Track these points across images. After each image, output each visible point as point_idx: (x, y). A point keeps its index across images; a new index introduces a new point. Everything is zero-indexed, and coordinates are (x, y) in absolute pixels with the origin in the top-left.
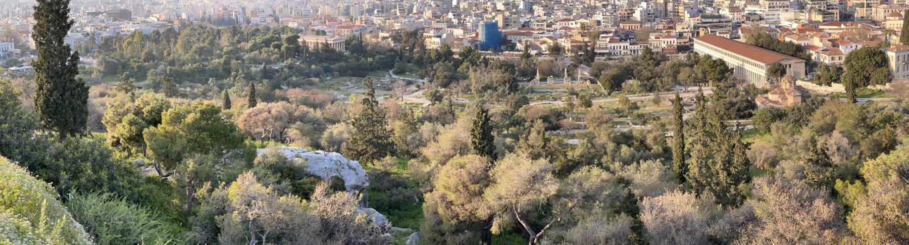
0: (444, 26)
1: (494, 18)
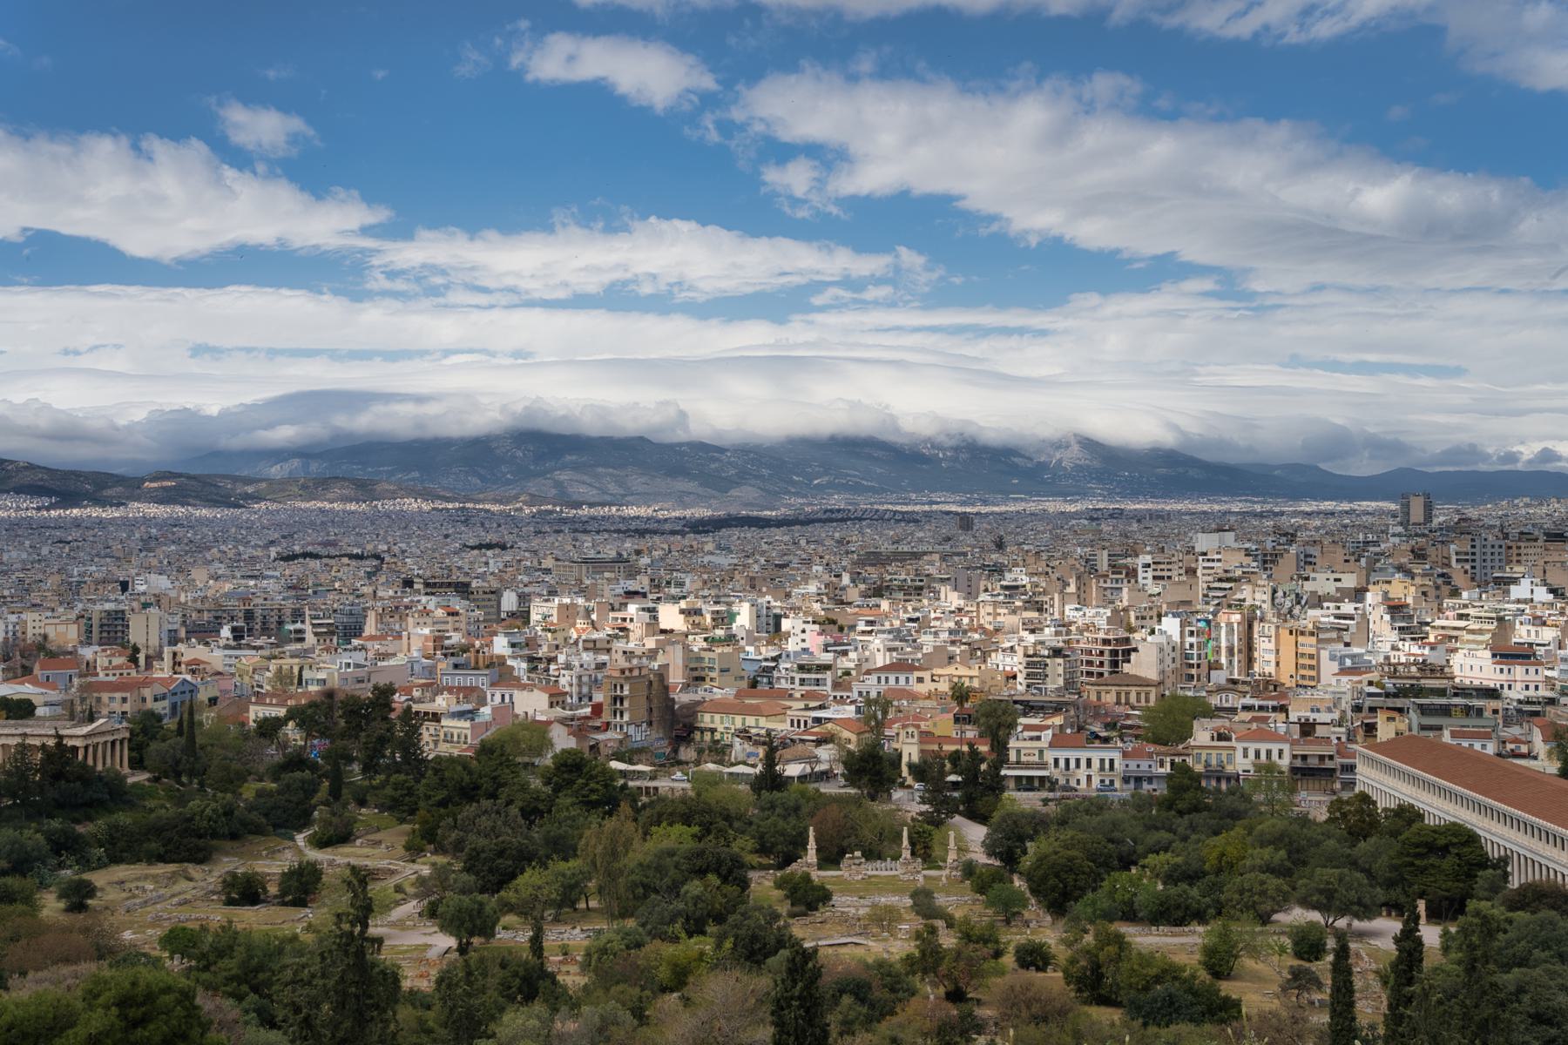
0: (481, 680)
1: (652, 655)
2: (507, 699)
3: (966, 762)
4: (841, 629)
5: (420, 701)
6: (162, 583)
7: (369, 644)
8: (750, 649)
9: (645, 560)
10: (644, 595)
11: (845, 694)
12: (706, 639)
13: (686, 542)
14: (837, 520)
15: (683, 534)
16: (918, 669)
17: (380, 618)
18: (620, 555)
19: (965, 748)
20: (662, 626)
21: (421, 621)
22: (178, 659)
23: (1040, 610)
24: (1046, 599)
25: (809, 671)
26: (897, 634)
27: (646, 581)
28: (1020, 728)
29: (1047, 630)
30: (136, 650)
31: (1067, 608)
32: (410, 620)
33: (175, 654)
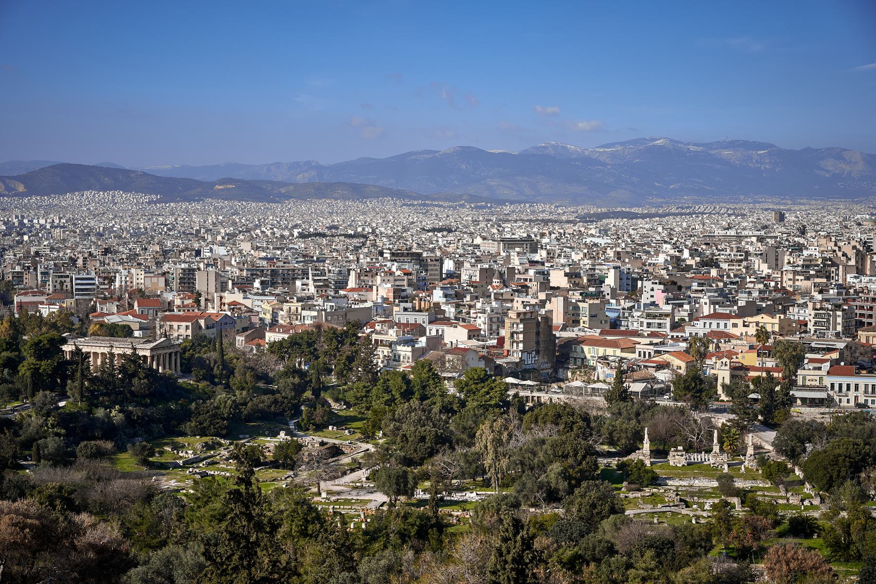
0: (422, 318)
1: (543, 303)
2: (440, 333)
3: (765, 384)
4: (680, 288)
5: (379, 333)
6: (221, 251)
7: (350, 294)
8: (613, 301)
9: (545, 240)
10: (543, 264)
11: (680, 334)
12: (581, 294)
13: (576, 228)
14: (686, 214)
15: (574, 223)
16: (733, 317)
17: (359, 276)
18: (529, 236)
19: (764, 375)
20: (552, 285)
21: (386, 278)
22: (223, 301)
23: (828, 277)
24: (833, 269)
25: (655, 317)
26: (721, 292)
27: (544, 253)
28: (806, 361)
29: (831, 292)
30: (200, 295)
31: (848, 276)
32: (379, 278)
33: (221, 298)
